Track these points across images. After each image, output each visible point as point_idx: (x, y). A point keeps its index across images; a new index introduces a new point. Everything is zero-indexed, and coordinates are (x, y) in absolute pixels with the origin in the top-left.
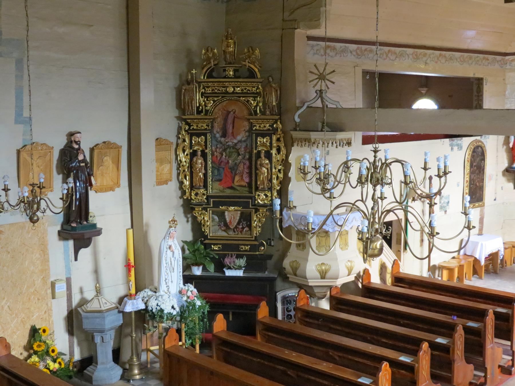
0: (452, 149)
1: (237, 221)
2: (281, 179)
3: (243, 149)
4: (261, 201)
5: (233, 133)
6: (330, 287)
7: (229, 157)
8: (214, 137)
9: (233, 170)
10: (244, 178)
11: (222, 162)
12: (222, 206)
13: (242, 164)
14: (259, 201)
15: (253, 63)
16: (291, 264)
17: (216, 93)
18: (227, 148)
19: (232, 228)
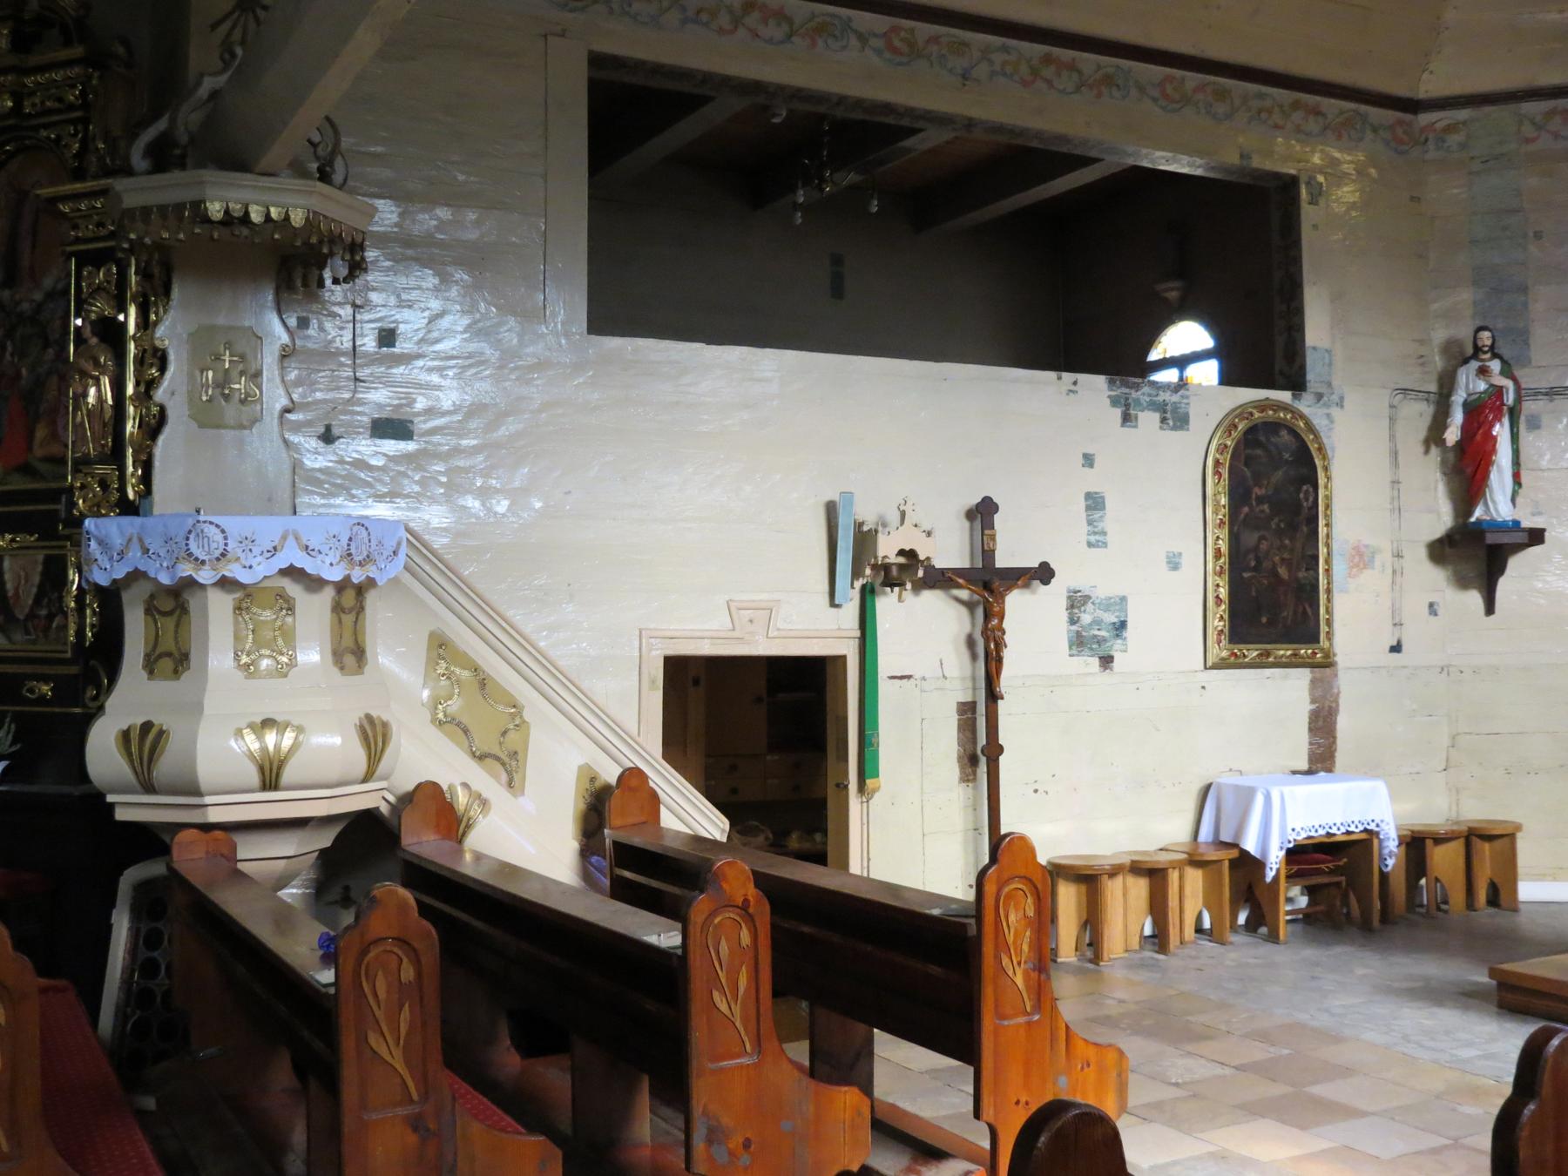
0: (1127, 419)
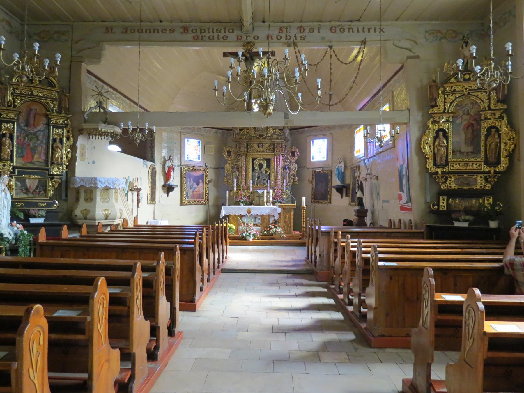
0: (144, 166)
1: (36, 186)
2: (70, 158)
3: (41, 136)
4: (55, 172)
5: (34, 125)
6: (110, 225)
7: (31, 141)
8: (19, 126)
9: (33, 150)
10: (42, 157)
11: (24, 144)
12: (25, 175)
13: (40, 147)
14: (53, 172)
15: (54, 77)
16: (82, 212)
17: (23, 94)
18: (29, 135)
19: (31, 191)
